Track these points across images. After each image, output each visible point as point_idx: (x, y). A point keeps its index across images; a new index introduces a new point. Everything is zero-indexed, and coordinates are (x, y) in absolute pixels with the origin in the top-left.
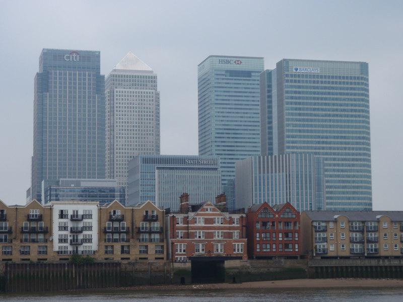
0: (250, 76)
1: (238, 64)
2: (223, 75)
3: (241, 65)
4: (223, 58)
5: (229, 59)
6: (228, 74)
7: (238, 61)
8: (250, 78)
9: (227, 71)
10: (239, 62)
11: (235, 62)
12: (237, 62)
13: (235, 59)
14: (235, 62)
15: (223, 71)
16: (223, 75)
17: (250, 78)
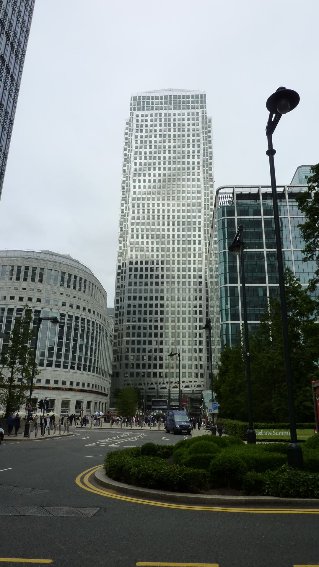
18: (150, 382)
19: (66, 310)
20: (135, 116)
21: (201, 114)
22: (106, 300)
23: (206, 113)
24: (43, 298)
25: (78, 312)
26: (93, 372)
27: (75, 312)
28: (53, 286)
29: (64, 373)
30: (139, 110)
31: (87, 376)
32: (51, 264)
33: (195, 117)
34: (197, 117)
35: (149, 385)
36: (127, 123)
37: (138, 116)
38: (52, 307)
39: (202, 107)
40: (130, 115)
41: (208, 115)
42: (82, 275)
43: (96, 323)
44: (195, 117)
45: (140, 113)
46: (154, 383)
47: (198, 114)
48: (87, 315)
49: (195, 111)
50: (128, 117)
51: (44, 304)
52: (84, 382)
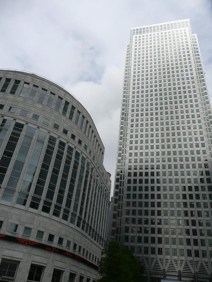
18: (155, 260)
19: (38, 124)
22: (103, 153)
24: (7, 104)
25: (55, 132)
26: (72, 221)
27: (51, 130)
28: (28, 100)
29: (17, 212)
31: (60, 226)
32: (30, 78)
35: (154, 263)
38: (17, 117)
42: (69, 99)
43: (83, 157)
46: (159, 261)
48: (69, 140)
51: (6, 112)
52: (53, 234)
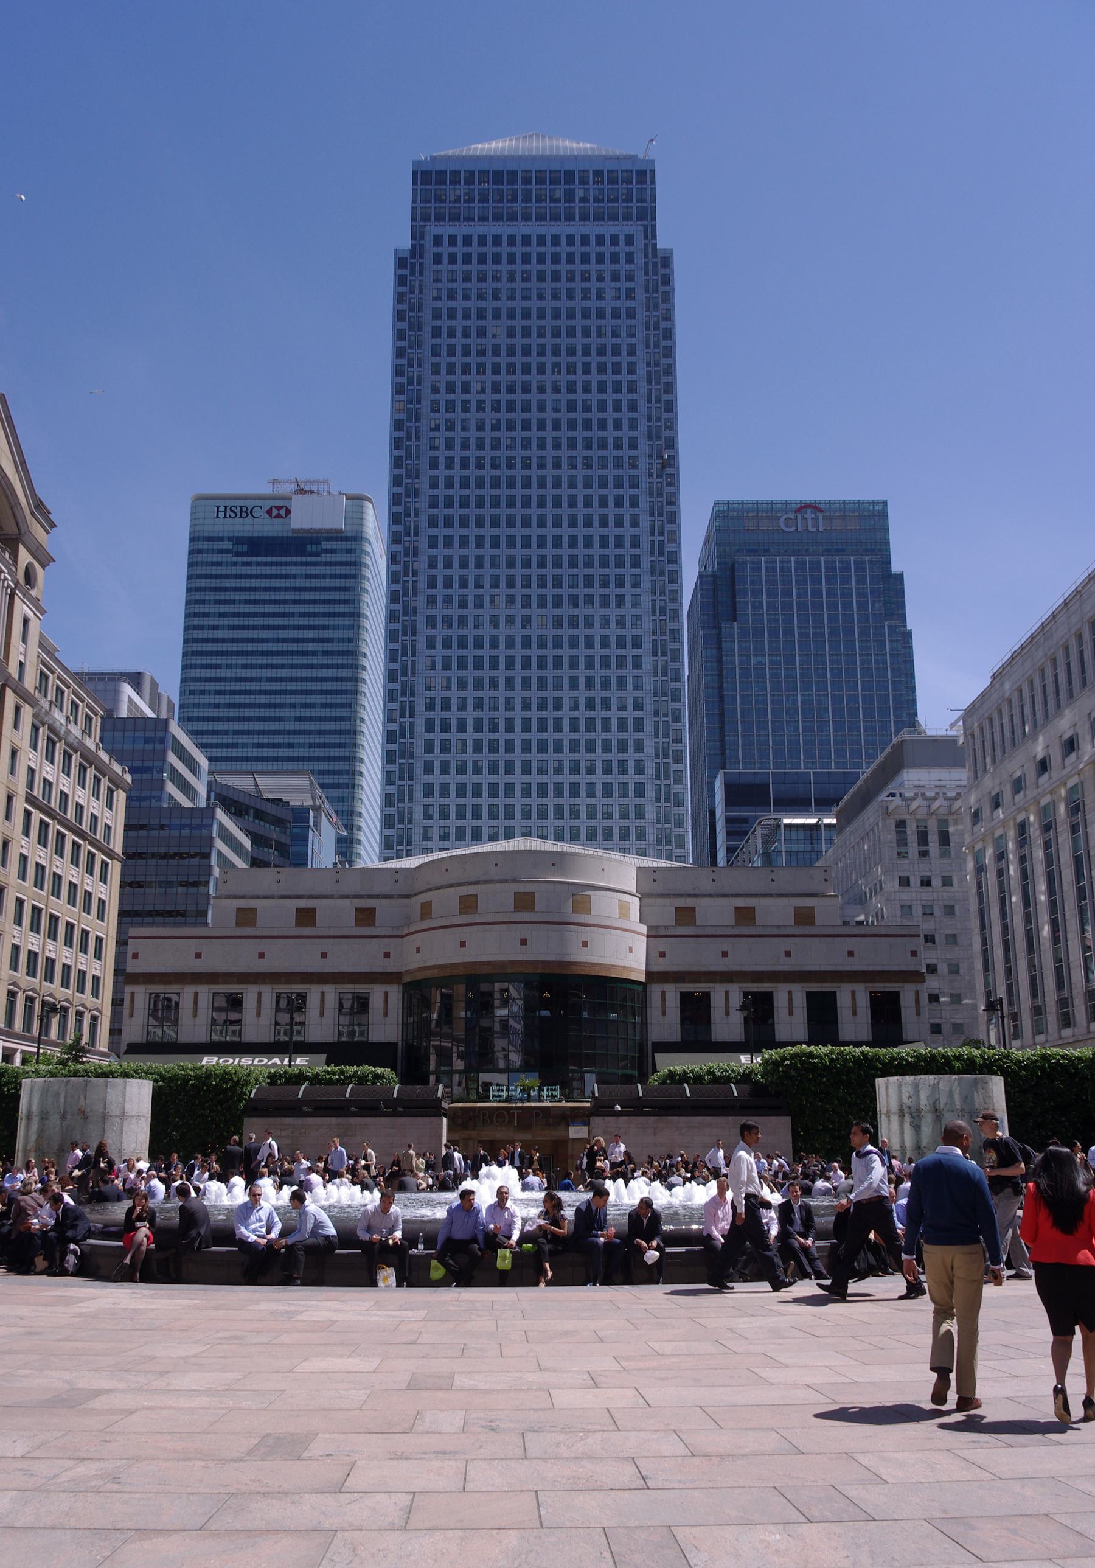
0: (318, 555)
1: (279, 516)
2: (227, 551)
3: (287, 520)
4: (230, 503)
5: (250, 504)
6: (245, 548)
7: (279, 508)
8: (318, 559)
9: (239, 541)
10: (283, 512)
11: (269, 512)
12: (275, 512)
13: (268, 504)
14: (269, 512)
15: (230, 539)
16: (227, 551)
17: (318, 559)
20: (429, 241)
21: (640, 241)
23: (655, 237)
30: (440, 218)
33: (622, 249)
34: (628, 249)
36: (401, 262)
37: (438, 241)
39: (642, 216)
40: (413, 238)
41: (662, 243)
44: (622, 249)
45: (446, 230)
47: (630, 240)
49: (621, 229)
50: (406, 244)
